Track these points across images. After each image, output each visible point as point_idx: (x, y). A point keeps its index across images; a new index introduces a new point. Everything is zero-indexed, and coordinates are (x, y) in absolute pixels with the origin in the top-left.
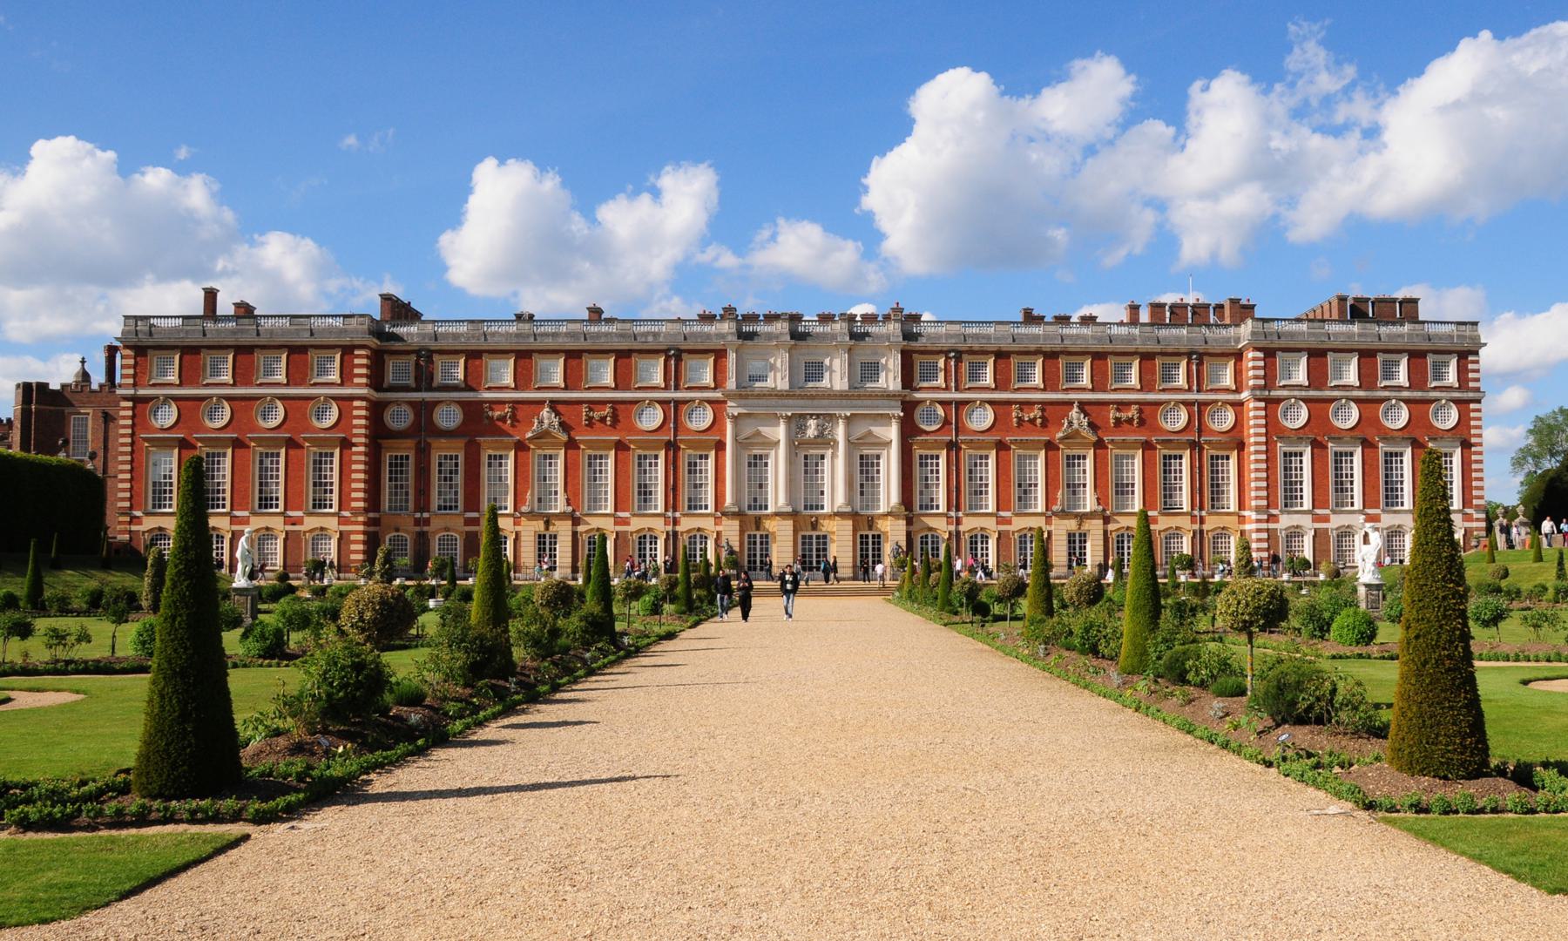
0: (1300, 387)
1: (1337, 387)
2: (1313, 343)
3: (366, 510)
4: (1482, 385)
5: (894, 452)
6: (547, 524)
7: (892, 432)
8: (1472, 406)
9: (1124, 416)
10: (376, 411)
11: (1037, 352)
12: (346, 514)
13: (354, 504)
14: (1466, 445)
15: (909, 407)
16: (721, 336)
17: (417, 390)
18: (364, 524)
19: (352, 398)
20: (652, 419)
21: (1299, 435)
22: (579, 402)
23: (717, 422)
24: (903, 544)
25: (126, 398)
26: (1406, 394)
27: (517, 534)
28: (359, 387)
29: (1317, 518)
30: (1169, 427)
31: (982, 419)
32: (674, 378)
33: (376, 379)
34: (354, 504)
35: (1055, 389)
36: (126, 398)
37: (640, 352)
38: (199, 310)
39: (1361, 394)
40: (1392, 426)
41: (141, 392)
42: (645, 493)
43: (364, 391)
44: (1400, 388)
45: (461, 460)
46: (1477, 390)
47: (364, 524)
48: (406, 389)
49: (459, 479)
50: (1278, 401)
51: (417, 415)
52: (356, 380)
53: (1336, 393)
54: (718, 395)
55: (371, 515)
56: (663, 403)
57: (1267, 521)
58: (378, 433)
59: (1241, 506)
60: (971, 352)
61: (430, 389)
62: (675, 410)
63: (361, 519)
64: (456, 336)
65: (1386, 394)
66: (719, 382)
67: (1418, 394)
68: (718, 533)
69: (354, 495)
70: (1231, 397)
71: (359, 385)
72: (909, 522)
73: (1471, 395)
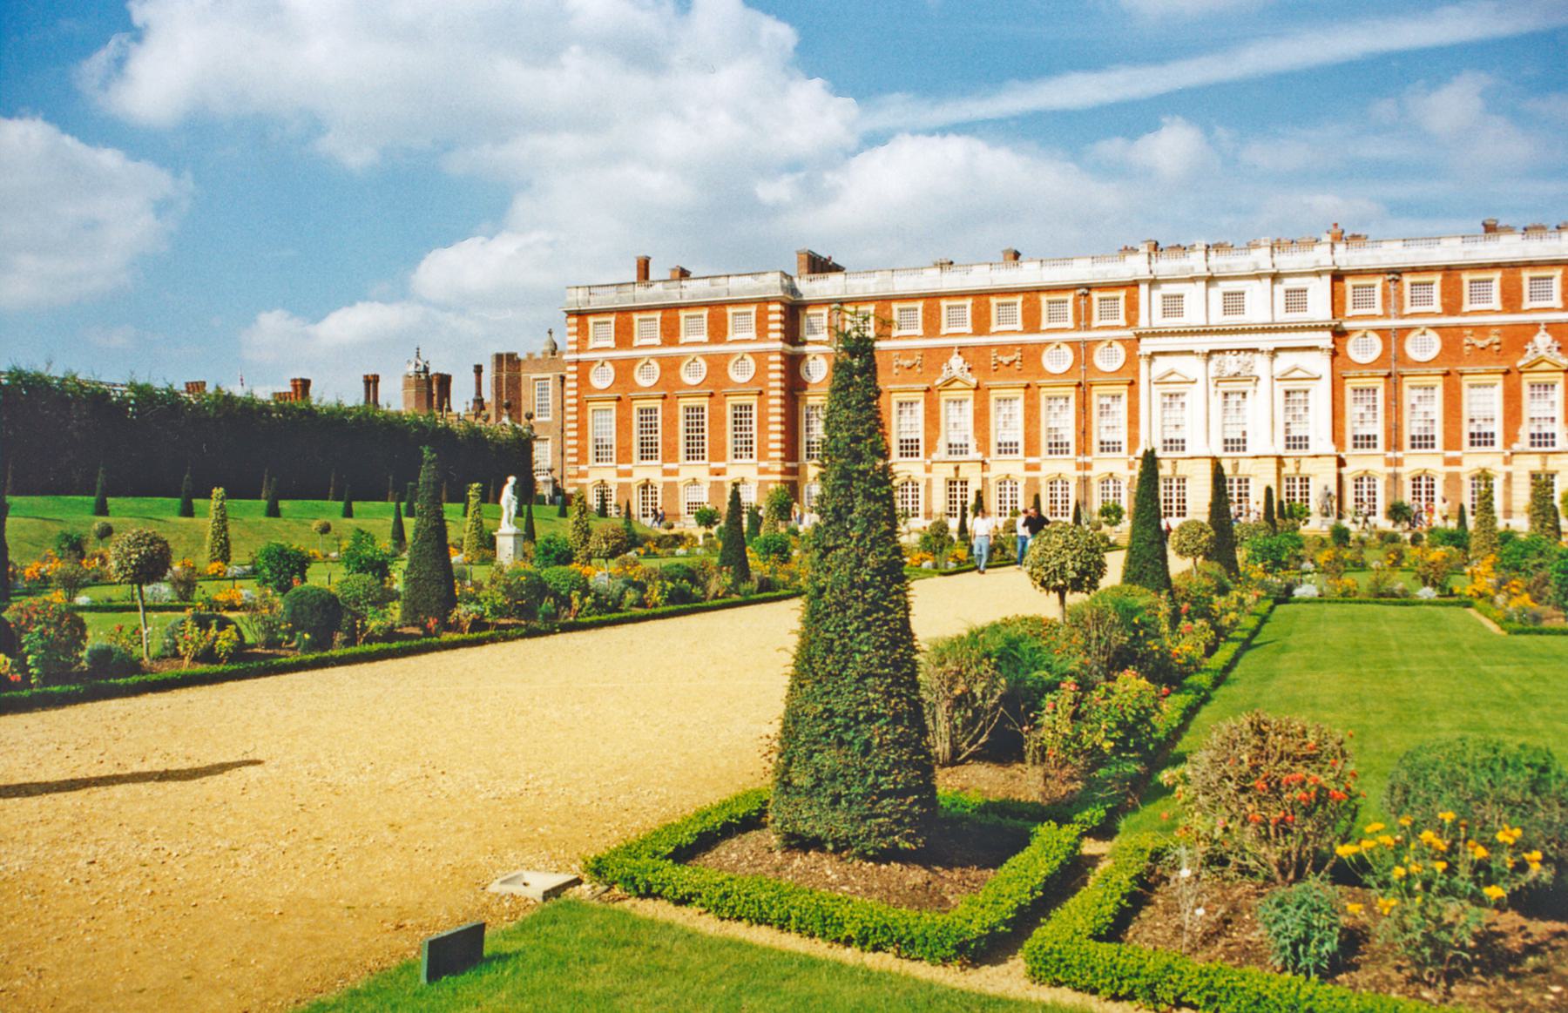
6: (957, 469)
7: (1320, 364)
12: (764, 464)
13: (772, 455)
15: (1339, 334)
18: (782, 473)
19: (769, 352)
20: (1057, 361)
23: (1132, 359)
24: (1333, 489)
25: (570, 363)
28: (775, 343)
34: (772, 455)
36: (570, 363)
41: (583, 356)
47: (782, 473)
54: (1129, 334)
55: (789, 464)
60: (1414, 270)
62: (1083, 351)
66: (1132, 320)
69: (772, 446)
71: (773, 340)
72: (1341, 463)
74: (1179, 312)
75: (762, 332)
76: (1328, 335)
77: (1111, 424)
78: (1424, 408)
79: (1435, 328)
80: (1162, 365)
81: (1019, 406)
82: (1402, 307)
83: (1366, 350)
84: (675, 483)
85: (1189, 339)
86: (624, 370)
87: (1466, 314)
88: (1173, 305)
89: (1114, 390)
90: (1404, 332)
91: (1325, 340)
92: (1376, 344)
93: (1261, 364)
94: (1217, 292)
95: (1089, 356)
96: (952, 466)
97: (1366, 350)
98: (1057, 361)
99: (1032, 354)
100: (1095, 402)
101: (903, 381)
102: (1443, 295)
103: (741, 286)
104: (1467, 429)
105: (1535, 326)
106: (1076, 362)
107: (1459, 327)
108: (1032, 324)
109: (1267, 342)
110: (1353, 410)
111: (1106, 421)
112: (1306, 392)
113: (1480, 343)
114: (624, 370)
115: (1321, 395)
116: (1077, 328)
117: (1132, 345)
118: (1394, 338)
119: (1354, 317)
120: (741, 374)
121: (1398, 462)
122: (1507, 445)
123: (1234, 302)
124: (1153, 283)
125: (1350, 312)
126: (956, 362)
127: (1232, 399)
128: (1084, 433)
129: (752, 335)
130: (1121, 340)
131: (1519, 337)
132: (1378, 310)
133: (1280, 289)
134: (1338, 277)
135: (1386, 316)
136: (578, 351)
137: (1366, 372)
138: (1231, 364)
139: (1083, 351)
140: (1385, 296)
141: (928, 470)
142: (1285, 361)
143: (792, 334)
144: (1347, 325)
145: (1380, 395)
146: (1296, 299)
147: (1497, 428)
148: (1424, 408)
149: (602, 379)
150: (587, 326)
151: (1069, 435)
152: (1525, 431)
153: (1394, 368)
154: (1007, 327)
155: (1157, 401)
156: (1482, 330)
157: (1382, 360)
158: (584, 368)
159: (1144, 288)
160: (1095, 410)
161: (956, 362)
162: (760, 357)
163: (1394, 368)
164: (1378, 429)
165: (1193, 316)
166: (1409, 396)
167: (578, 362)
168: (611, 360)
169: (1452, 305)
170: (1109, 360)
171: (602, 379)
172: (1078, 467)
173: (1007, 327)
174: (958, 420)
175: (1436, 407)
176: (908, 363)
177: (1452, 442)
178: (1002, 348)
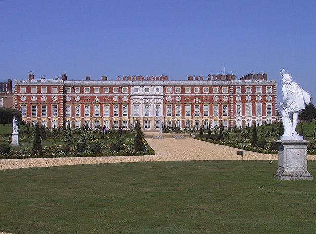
1: (247, 93)
5: (163, 104)
7: (162, 101)
14: (273, 104)
15: (165, 96)
17: (72, 94)
19: (61, 96)
20: (116, 99)
21: (240, 102)
24: (164, 123)
27: (91, 121)
29: (243, 118)
31: (178, 99)
35: (193, 93)
49: (80, 111)
51: (71, 98)
60: (177, 86)
62: (121, 98)
72: (165, 118)
74: (137, 91)
75: (59, 92)
77: (125, 111)
78: (179, 109)
79: (180, 96)
81: (108, 107)
86: (29, 98)
88: (136, 90)
89: (126, 105)
91: (162, 97)
92: (171, 98)
93: (151, 101)
94: (144, 88)
95: (122, 98)
97: (169, 99)
98: (116, 99)
99: (111, 97)
100: (123, 107)
103: (54, 81)
104: (185, 113)
108: (111, 92)
110: (167, 109)
115: (162, 107)
116: (119, 93)
118: (174, 97)
120: (55, 99)
121: (175, 118)
123: (147, 90)
124: (133, 86)
126: (97, 99)
128: (121, 112)
133: (155, 88)
134: (164, 86)
139: (121, 98)
141: (91, 119)
142: (156, 101)
143: (64, 92)
146: (158, 90)
147: (190, 113)
148: (179, 109)
151: (118, 113)
152: (195, 113)
153: (174, 102)
154: (107, 92)
155: (134, 107)
156: (188, 96)
158: (19, 97)
159: (131, 87)
160: (123, 108)
161: (97, 99)
162: (59, 97)
163: (174, 102)
164: (171, 113)
166: (176, 107)
169: (183, 92)
170: (125, 99)
171: (23, 99)
173: (107, 92)
174: (97, 110)
175: (180, 109)
177: (183, 115)
178: (105, 96)
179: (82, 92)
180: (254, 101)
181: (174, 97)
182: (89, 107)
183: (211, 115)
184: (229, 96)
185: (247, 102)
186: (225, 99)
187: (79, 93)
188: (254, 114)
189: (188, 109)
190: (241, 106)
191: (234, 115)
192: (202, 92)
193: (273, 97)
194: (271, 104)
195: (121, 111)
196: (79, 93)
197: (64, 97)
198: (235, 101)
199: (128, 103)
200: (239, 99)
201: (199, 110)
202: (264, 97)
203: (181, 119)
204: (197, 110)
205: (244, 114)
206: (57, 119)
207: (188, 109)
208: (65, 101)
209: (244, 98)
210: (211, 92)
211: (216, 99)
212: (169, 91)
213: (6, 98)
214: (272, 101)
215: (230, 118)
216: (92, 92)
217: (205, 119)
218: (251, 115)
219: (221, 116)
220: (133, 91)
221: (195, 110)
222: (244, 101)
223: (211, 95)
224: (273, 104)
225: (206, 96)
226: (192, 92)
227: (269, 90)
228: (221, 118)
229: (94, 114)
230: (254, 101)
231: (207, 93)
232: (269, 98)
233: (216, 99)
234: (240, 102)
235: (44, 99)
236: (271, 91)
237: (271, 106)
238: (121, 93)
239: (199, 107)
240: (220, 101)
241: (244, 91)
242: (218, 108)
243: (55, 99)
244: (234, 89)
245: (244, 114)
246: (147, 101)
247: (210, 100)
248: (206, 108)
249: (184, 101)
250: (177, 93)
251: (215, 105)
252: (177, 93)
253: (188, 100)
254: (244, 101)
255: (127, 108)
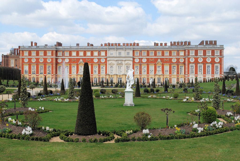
0: (193, 56)
1: (200, 56)
2: (196, 49)
3: (55, 74)
4: (224, 55)
5: (132, 65)
7: (131, 63)
8: (222, 58)
9: (167, 60)
10: (57, 59)
11: (153, 50)
13: (54, 73)
14: (221, 65)
15: (134, 59)
16: (106, 49)
17: (62, 57)
21: (193, 63)
22: (86, 58)
26: (211, 57)
30: (173, 62)
31: (144, 61)
32: (99, 54)
33: (56, 55)
34: (54, 73)
37: (94, 51)
38: (30, 45)
39: (203, 57)
40: (208, 62)
41: (23, 57)
42: (95, 72)
43: (55, 57)
44: (210, 56)
45: (69, 67)
46: (223, 56)
48: (61, 56)
49: (69, 69)
50: (190, 58)
52: (54, 55)
53: (199, 57)
54: (105, 57)
56: (98, 58)
57: (187, 76)
58: (57, 63)
59: (185, 74)
61: (64, 56)
63: (55, 75)
64: (68, 49)
65: (207, 57)
67: (213, 57)
68: (106, 77)
70: (183, 57)
73: (222, 57)
75: (52, 55)
76: (132, 58)
78: (144, 67)
79: (146, 58)
80: (110, 62)
82: (142, 55)
83: (137, 61)
84: (38, 77)
85: (114, 58)
86: (30, 60)
87: (150, 56)
90: (142, 58)
91: (132, 59)
93: (123, 62)
94: (118, 52)
96: (80, 75)
97: (137, 61)
98: (96, 61)
100: (101, 66)
101: (73, 63)
102: (147, 54)
105: (158, 58)
106: (98, 61)
107: (149, 58)
109: (124, 59)
111: (103, 69)
112: (129, 66)
113: (151, 60)
114: (30, 60)
117: (106, 59)
118: (141, 59)
119: (136, 56)
120: (49, 61)
121: (141, 76)
122: (155, 74)
123: (120, 53)
125: (135, 55)
126: (81, 60)
127: (120, 67)
129: (51, 55)
130: (105, 58)
131: (156, 60)
132: (139, 55)
134: (133, 51)
135: (140, 56)
136: (22, 56)
137: (137, 64)
138: (120, 62)
140: (140, 53)
141: (77, 76)
142: (126, 62)
143: (56, 55)
144: (135, 57)
145: (139, 67)
146: (128, 53)
148: (144, 67)
149: (26, 61)
150: (24, 52)
155: (110, 67)
156: (152, 59)
157: (139, 62)
160: (101, 68)
161: (81, 60)
162: (52, 59)
165: (114, 55)
166: (142, 67)
167: (22, 58)
168: (28, 58)
169: (148, 55)
170: (103, 61)
171: (26, 61)
172: (98, 76)
175: (146, 69)
176: (74, 60)
179: (70, 55)
180: (205, 62)
181: (141, 59)
182: (76, 67)
183: (170, 73)
184: (185, 59)
185: (199, 63)
186: (182, 61)
187: (68, 56)
188: (204, 73)
189: (152, 67)
190: (194, 67)
191: (188, 74)
192: (163, 55)
193: (221, 59)
194: (219, 65)
195: (100, 70)
196: (68, 56)
197: (57, 59)
198: (189, 62)
199: (106, 62)
200: (192, 60)
201: (161, 70)
202: (213, 60)
203: (146, 76)
204: (159, 69)
205: (196, 73)
206: (50, 76)
207: (152, 67)
208: (57, 63)
209: (196, 60)
210: (170, 55)
211: (174, 61)
212: (137, 54)
213: (16, 60)
214: (220, 62)
215: (185, 76)
216: (78, 54)
217: (165, 76)
218: (202, 74)
219: (178, 74)
220: (109, 53)
221: (158, 69)
222: (196, 62)
223: (171, 57)
224: (221, 65)
225: (166, 58)
226: (155, 55)
227: (217, 53)
228: (178, 76)
229: (79, 72)
230: (205, 62)
231: (167, 56)
232: (217, 60)
233: (174, 61)
234: (193, 63)
235: (41, 61)
236: (219, 54)
237: (219, 67)
238: (100, 56)
239: (161, 67)
240: (178, 62)
241: (196, 53)
242: (176, 68)
243: (49, 61)
244: (189, 52)
245: (196, 73)
246: (120, 62)
247: (170, 61)
248: (167, 67)
249: (149, 61)
250: (143, 56)
251: (174, 65)
252: (143, 56)
253: (152, 62)
254: (196, 62)
255: (105, 68)
